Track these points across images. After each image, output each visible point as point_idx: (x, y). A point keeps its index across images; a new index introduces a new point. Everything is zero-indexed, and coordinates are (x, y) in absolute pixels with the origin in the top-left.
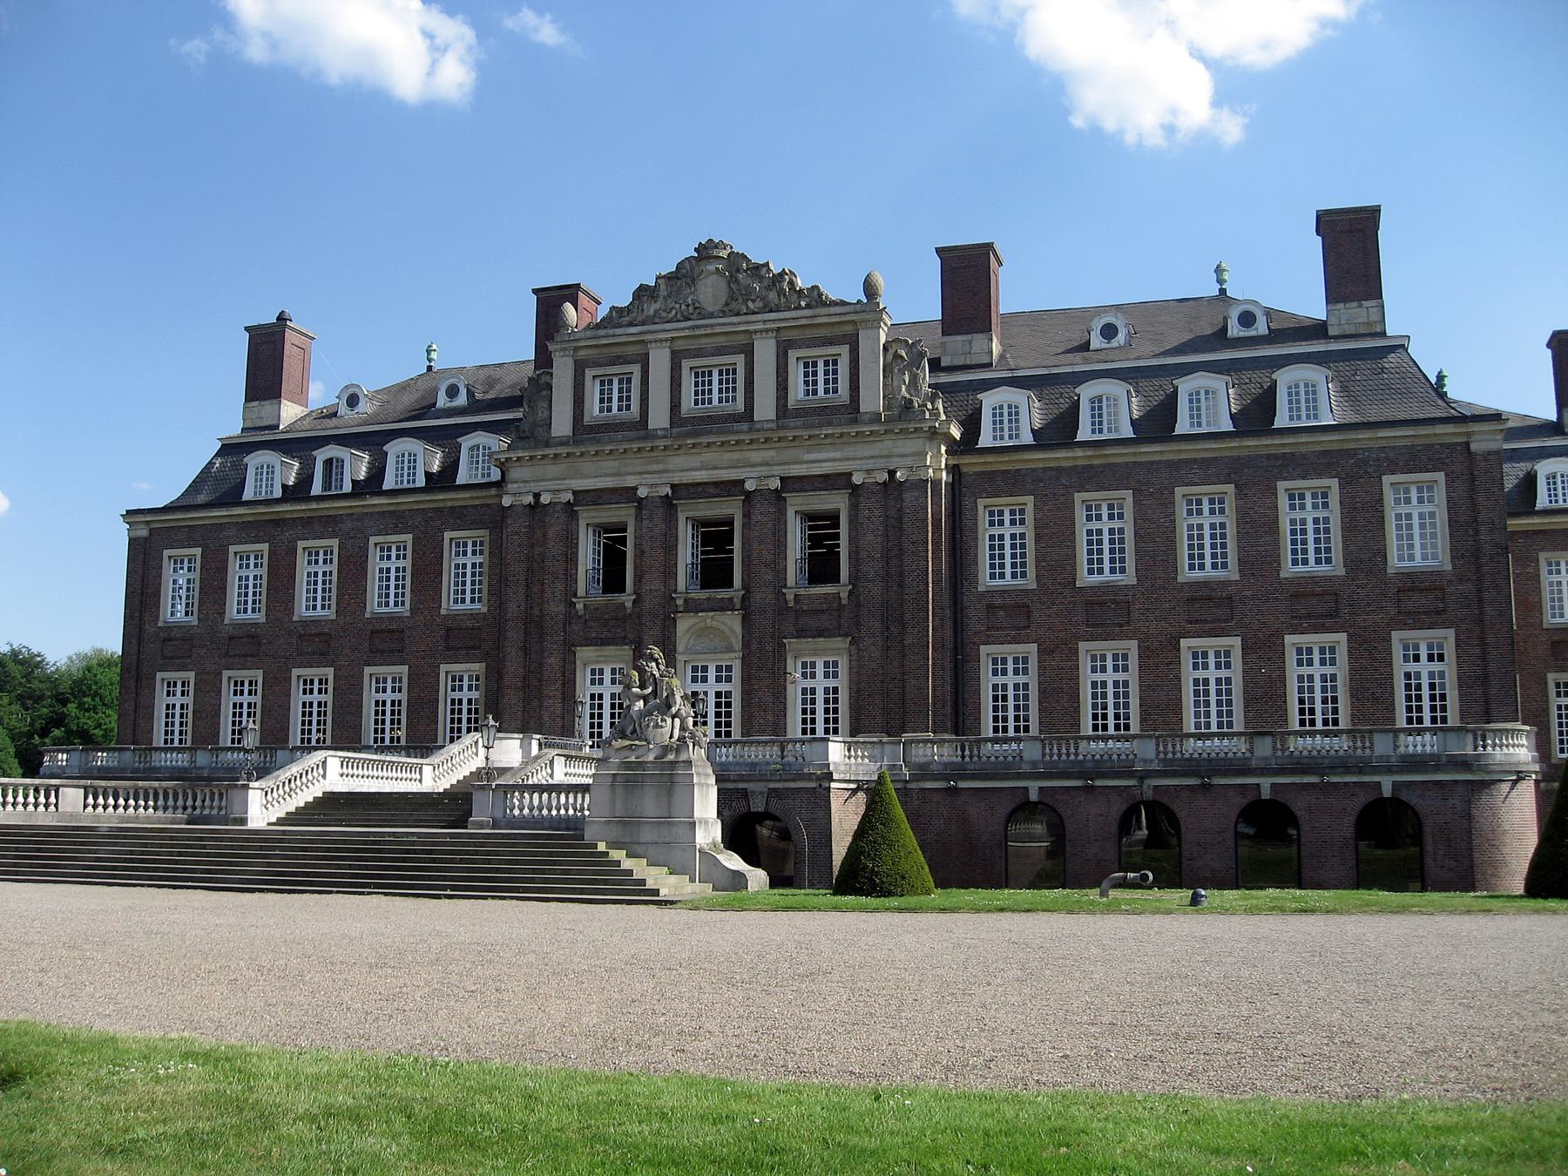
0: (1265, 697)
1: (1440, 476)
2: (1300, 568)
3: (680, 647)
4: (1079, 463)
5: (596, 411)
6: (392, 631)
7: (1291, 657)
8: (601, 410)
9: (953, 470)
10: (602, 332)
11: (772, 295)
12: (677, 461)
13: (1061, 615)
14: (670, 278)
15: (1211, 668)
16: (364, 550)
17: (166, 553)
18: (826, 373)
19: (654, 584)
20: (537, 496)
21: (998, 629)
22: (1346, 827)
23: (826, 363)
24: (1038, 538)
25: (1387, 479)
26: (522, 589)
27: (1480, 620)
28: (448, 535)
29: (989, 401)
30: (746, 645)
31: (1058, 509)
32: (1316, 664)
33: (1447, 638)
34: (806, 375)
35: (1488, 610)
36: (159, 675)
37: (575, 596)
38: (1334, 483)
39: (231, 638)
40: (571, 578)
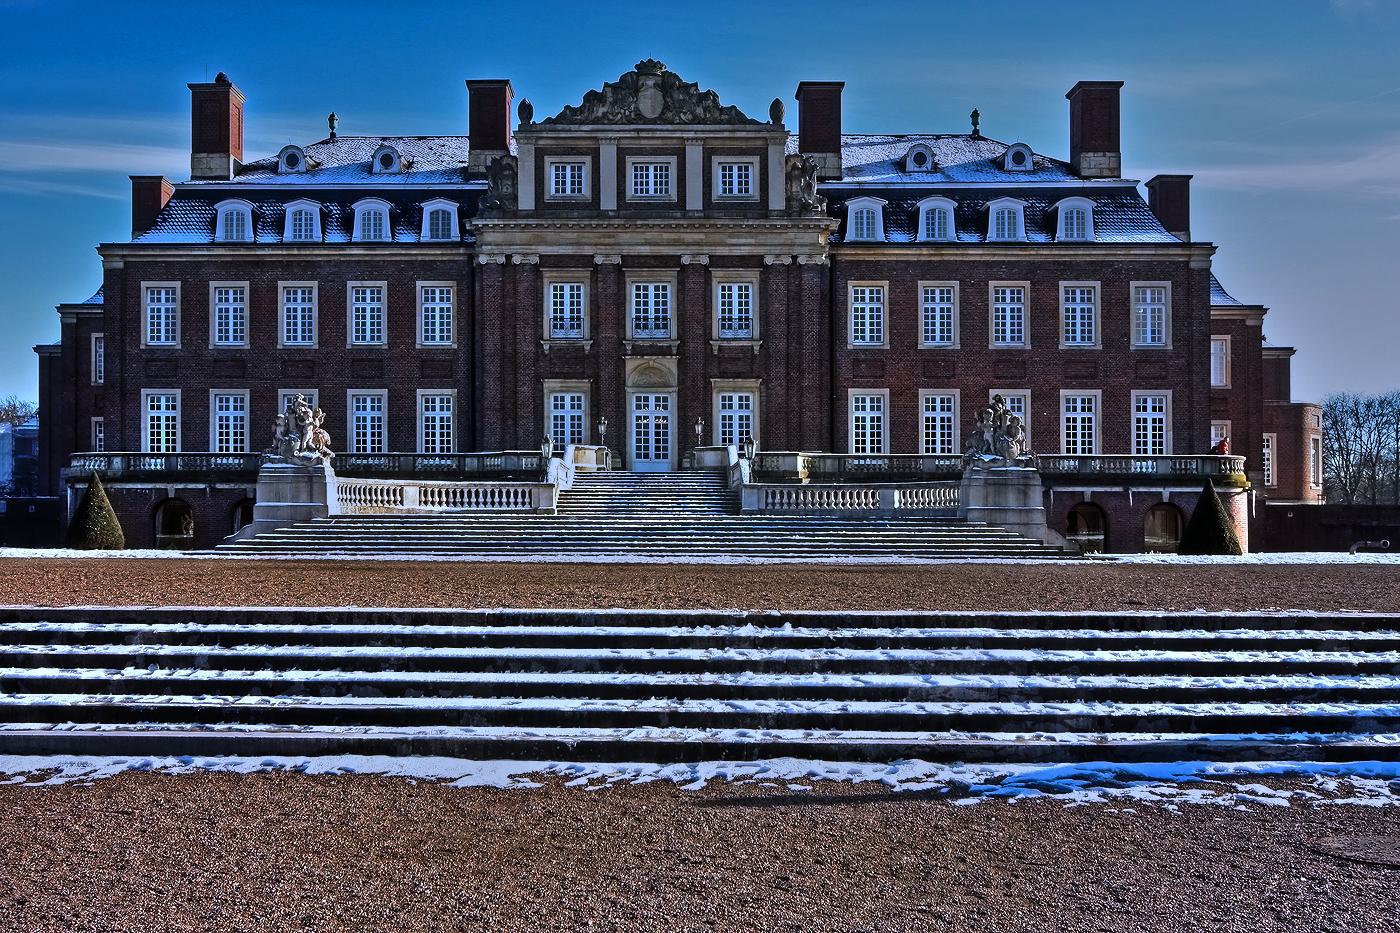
1: (1168, 284)
2: (1071, 343)
3: (629, 382)
4: (923, 258)
5: (553, 192)
6: (372, 360)
8: (557, 191)
9: (832, 257)
10: (560, 127)
12: (625, 237)
13: (904, 367)
14: (614, 87)
18: (740, 176)
20: (509, 257)
21: (862, 377)
23: (740, 169)
25: (1133, 284)
26: (497, 332)
28: (419, 284)
29: (853, 206)
30: (681, 382)
31: (906, 292)
34: (724, 176)
35: (1195, 377)
36: (144, 391)
37: (542, 339)
38: (1098, 284)
39: (216, 361)
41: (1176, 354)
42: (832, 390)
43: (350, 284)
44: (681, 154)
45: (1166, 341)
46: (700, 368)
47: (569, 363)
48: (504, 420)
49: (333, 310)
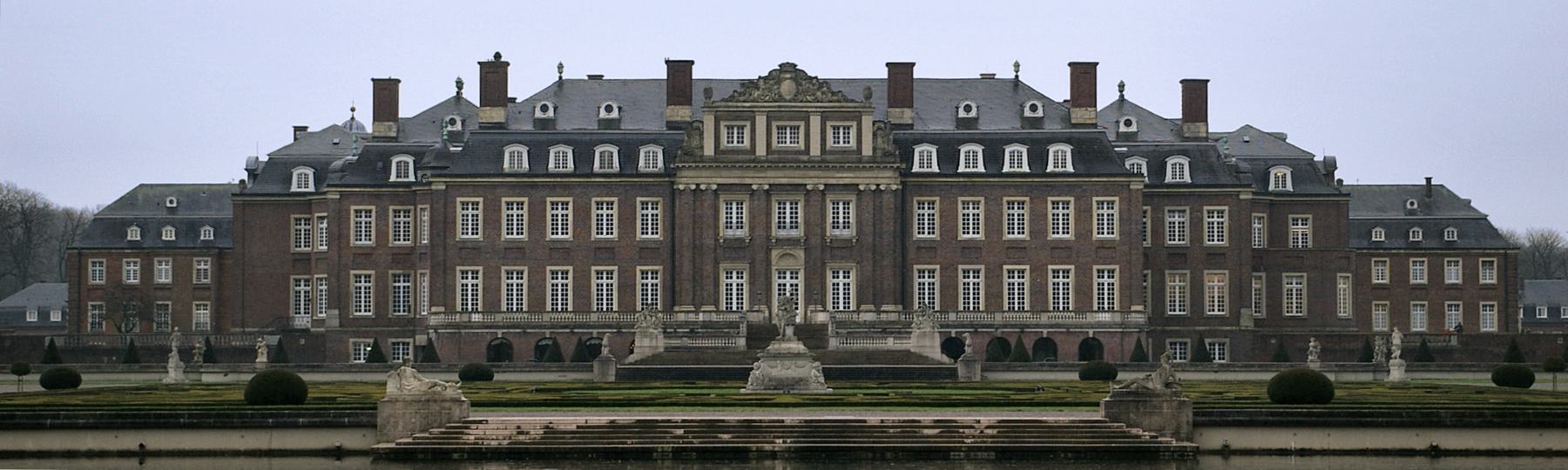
0: (1039, 292)
1: (1116, 199)
7: (1050, 274)
12: (771, 173)
15: (1017, 280)
17: (459, 199)
19: (760, 232)
22: (1076, 348)
27: (1129, 262)
28: (639, 199)
32: (1061, 279)
40: (717, 227)
41: (1122, 242)
42: (904, 266)
45: (1116, 236)
46: (821, 253)
47: (735, 249)
49: (582, 215)
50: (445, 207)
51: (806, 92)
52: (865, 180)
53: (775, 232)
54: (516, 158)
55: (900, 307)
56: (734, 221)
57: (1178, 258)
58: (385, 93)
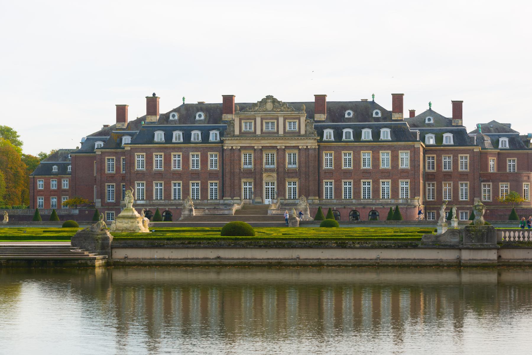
0: (376, 191)
1: (409, 151)
3: (264, 179)
9: (319, 145)
11: (282, 108)
12: (263, 142)
13: (339, 174)
15: (366, 185)
16: (189, 155)
17: (136, 154)
20: (232, 147)
24: (335, 159)
25: (400, 151)
27: (414, 178)
28: (209, 153)
32: (386, 185)
33: (409, 181)
36: (136, 182)
38: (390, 152)
40: (240, 164)
43: (190, 153)
44: (278, 120)
45: (409, 167)
47: (248, 173)
48: (231, 189)
49: (186, 160)
50: (130, 156)
51: (277, 108)
52: (302, 144)
53: (265, 166)
54: (159, 136)
55: (317, 198)
56: (246, 162)
57: (448, 176)
58: (121, 111)
